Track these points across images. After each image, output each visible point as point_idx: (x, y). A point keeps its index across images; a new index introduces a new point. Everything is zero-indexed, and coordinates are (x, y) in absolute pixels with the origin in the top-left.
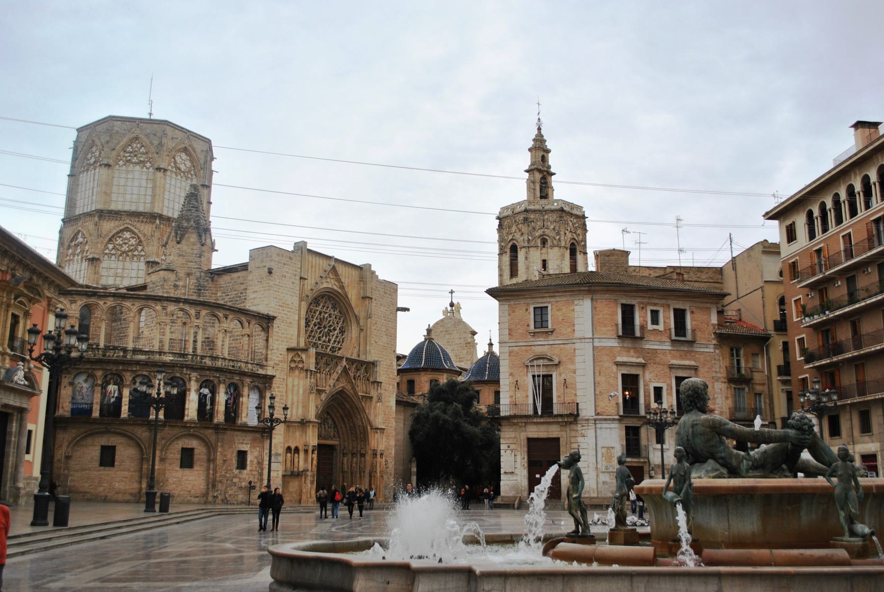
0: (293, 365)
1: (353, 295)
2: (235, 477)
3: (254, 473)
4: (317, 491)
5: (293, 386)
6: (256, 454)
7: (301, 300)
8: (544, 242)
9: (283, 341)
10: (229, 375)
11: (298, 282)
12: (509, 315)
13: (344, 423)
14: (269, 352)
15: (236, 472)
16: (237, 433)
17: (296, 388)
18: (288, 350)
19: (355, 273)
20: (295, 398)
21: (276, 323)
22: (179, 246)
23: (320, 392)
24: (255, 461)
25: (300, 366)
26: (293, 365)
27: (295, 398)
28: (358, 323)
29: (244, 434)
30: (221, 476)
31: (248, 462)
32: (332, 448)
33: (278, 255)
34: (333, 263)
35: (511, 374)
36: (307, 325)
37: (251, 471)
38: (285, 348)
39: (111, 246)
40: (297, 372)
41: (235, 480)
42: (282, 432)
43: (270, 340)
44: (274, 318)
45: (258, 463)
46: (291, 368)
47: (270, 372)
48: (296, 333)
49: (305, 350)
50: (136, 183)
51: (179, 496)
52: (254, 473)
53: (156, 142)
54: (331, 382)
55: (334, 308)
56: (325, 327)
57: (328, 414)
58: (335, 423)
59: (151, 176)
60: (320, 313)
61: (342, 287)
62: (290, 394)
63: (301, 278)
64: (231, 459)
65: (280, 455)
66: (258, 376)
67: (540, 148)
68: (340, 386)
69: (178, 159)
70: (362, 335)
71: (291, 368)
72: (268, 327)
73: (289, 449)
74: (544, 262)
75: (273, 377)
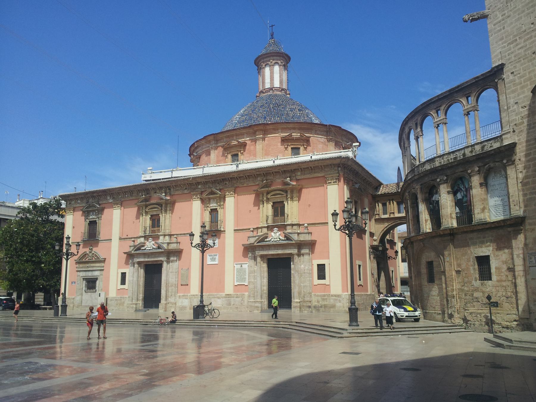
2: (477, 290)
3: (504, 284)
4: (38, 307)
9: (522, 88)
10: (449, 172)
16: (471, 235)
24: (505, 267)
31: (493, 270)
37: (498, 281)
41: (476, 294)
52: (504, 284)
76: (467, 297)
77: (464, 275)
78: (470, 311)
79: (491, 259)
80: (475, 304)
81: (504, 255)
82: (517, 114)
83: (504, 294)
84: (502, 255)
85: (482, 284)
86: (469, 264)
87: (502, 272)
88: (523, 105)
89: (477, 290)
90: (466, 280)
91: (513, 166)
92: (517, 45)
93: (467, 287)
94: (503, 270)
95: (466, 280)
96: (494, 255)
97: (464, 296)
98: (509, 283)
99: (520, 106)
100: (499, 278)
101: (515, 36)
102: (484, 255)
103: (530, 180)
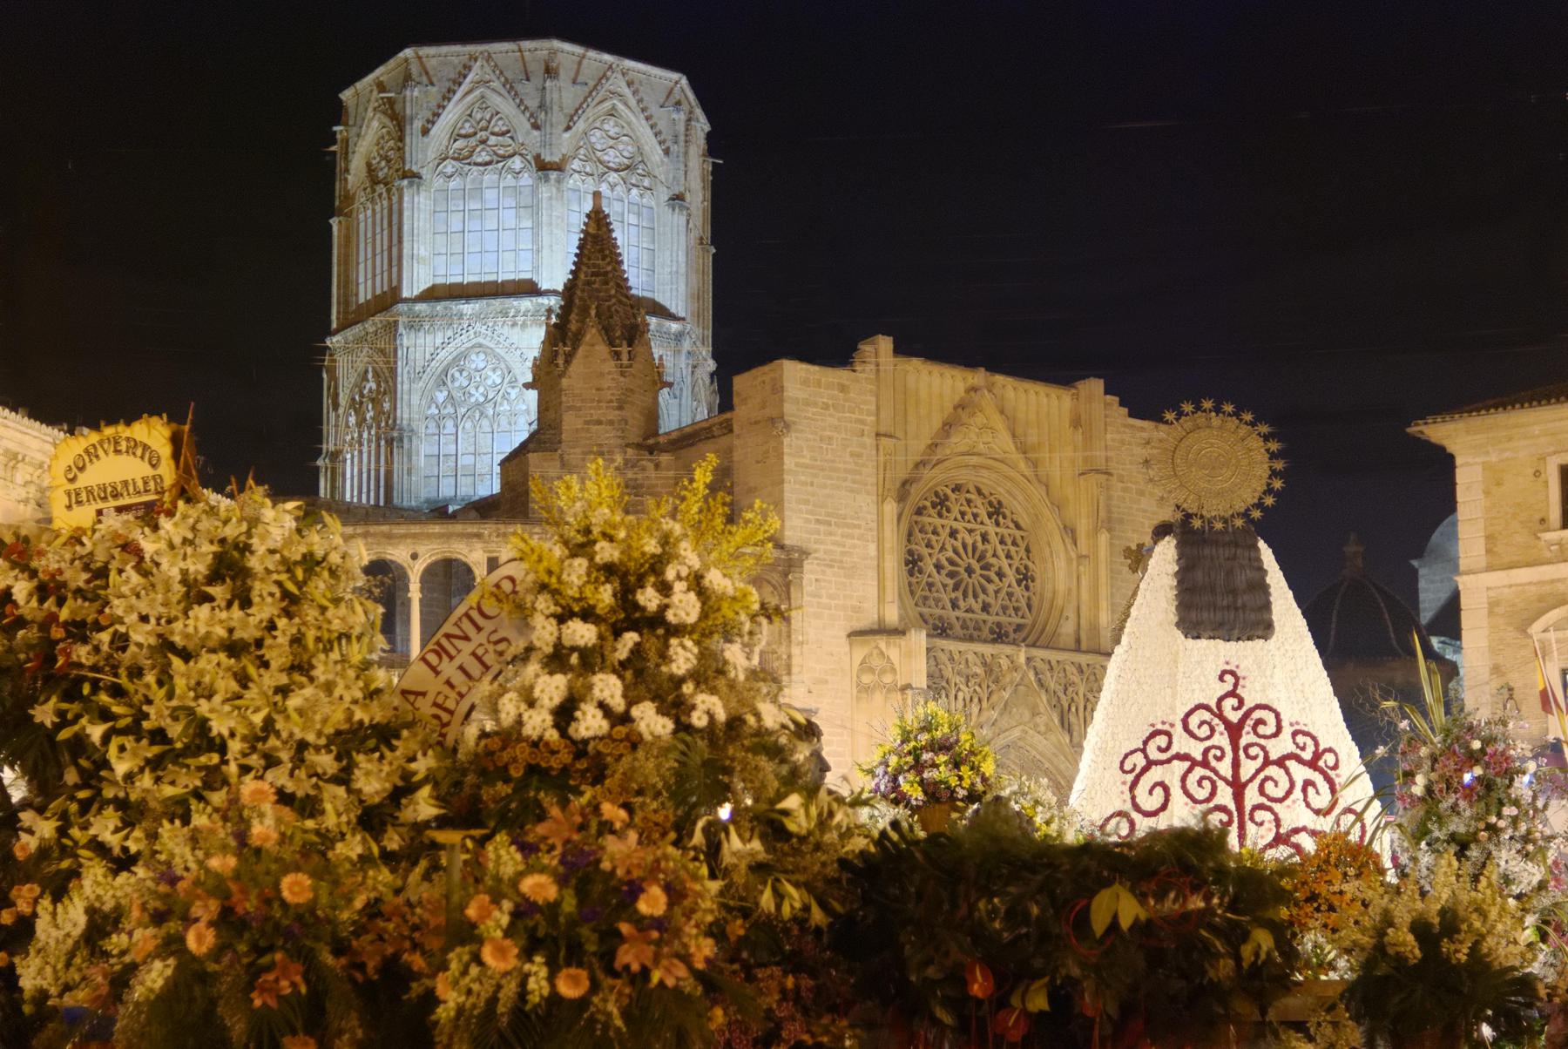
0: (867, 679)
7: (881, 499)
12: (1487, 493)
14: (795, 650)
22: (565, 382)
25: (888, 679)
26: (867, 679)
33: (806, 382)
35: (1496, 670)
36: (912, 563)
38: (843, 634)
39: (441, 396)
40: (878, 697)
48: (873, 592)
49: (898, 632)
50: (491, 223)
53: (533, 103)
56: (970, 571)
59: (526, 199)
60: (953, 534)
69: (596, 137)
71: (864, 690)
72: (788, 585)
92: (830, 534)
101: (828, 515)
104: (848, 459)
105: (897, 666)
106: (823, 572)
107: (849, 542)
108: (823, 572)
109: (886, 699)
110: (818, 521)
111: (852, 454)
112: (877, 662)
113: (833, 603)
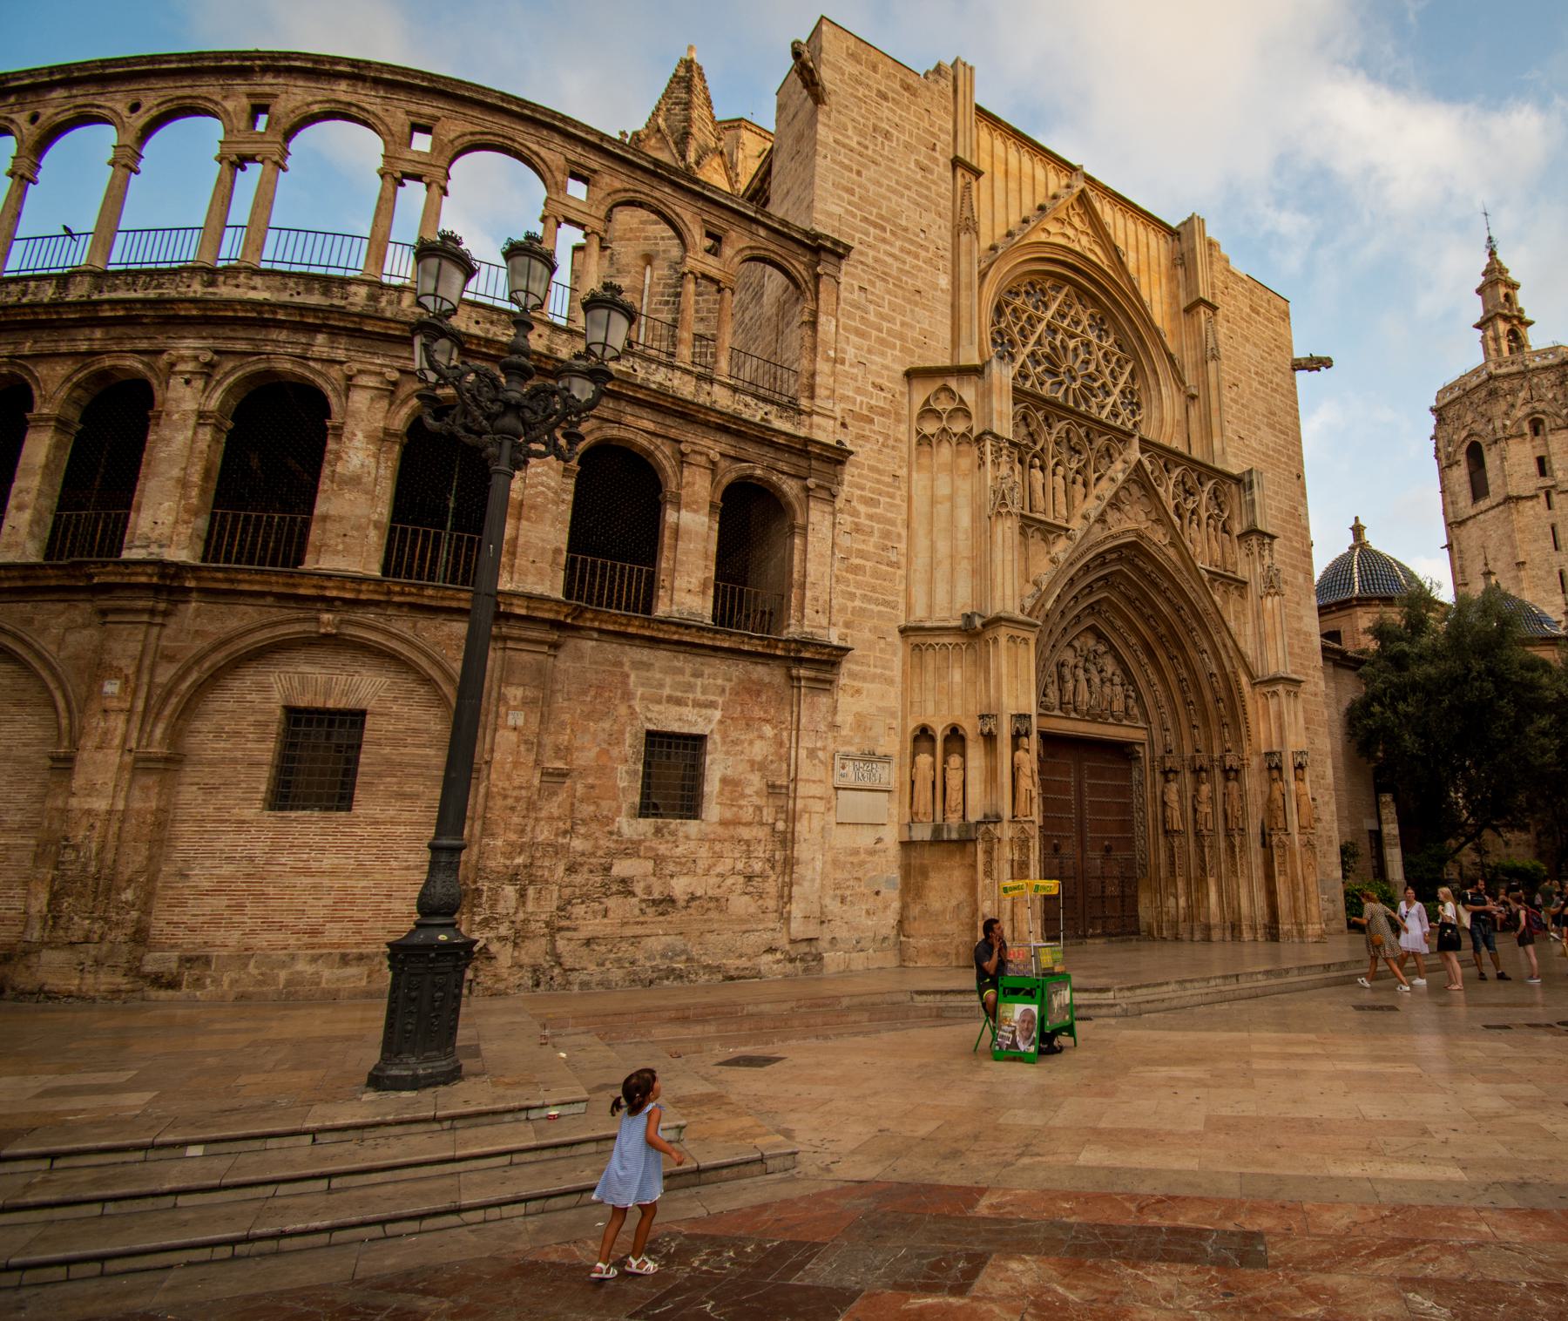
0: (930, 427)
1: (1157, 297)
2: (631, 850)
3: (746, 833)
5: (933, 502)
6: (759, 750)
8: (1536, 426)
11: (942, 169)
13: (1159, 670)
15: (633, 828)
16: (644, 654)
17: (943, 509)
18: (912, 375)
19: (1157, 246)
20: (943, 547)
21: (850, 275)
23: (1050, 531)
24: (756, 782)
25: (959, 427)
26: (930, 427)
27: (943, 547)
28: (1180, 380)
29: (680, 661)
30: (514, 849)
32: (1122, 751)
34: (1080, 184)
37: (724, 823)
41: (621, 868)
42: (896, 672)
43: (826, 325)
44: (839, 252)
45: (773, 789)
46: (924, 439)
47: (825, 432)
51: (244, 956)
52: (746, 833)
54: (1092, 507)
55: (1099, 324)
57: (1092, 629)
58: (1126, 671)
61: (1120, 263)
62: (920, 528)
63: (957, 163)
64: (603, 770)
65: (886, 759)
66: (762, 436)
67: (1495, 281)
68: (1133, 521)
70: (1194, 413)
71: (924, 439)
73: (923, 735)
74: (1541, 461)
75: (837, 457)
76: (578, 879)
77: (580, 789)
78: (583, 934)
79: (709, 746)
80: (611, 903)
81: (758, 744)
82: (858, 390)
83: (740, 866)
84: (751, 743)
85: (658, 831)
86: (615, 752)
87: (743, 796)
88: (878, 381)
89: (631, 850)
90: (587, 810)
91: (828, 509)
92: (884, 240)
93: (586, 837)
94: (748, 791)
95: (587, 810)
96: (724, 737)
97: (560, 871)
98: (762, 833)
99: (871, 379)
100: (728, 815)
101: (882, 217)
102: (685, 730)
103: (869, 564)
104: (912, 165)
105: (972, 410)
106: (873, 284)
107: (909, 259)
108: (873, 284)
109: (958, 454)
110: (865, 220)
111: (917, 162)
112: (944, 405)
113: (885, 325)
